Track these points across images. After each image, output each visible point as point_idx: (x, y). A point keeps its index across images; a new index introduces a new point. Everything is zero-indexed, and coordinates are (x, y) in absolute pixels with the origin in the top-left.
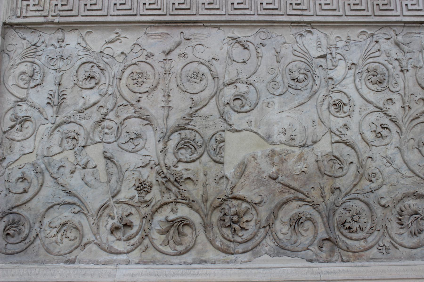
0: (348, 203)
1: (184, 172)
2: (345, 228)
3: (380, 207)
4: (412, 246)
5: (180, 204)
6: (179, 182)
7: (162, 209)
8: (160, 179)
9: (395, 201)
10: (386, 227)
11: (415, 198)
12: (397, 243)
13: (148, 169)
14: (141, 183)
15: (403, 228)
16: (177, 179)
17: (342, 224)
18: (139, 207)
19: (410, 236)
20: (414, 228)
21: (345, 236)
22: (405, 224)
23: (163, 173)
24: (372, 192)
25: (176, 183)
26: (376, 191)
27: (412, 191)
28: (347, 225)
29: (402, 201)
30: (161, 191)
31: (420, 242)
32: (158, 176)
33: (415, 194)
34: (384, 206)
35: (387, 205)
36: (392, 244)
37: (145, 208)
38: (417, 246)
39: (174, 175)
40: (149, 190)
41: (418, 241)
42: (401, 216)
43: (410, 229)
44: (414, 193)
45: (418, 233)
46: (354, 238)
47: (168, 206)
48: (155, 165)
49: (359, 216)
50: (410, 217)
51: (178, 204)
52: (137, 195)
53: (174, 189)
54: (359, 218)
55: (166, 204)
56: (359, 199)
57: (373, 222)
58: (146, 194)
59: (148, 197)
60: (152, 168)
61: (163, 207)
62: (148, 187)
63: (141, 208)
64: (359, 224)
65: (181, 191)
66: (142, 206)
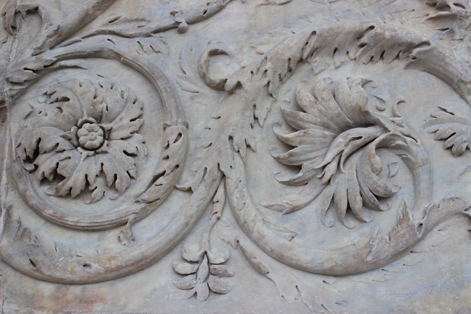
0: (70, 73)
2: (39, 174)
3: (207, 90)
4: (327, 265)
9: (269, 65)
10: (223, 176)
11: (365, 58)
12: (263, 249)
15: (303, 183)
17: (28, 160)
19: (330, 218)
20: (346, 184)
21: (37, 212)
22: (305, 165)
24: (175, 26)
26: (198, 27)
27: (351, 24)
28: (46, 163)
29: (305, 67)
31: (369, 246)
33: (364, 40)
34: (219, 87)
35: (230, 84)
36: (243, 251)
38: (352, 262)
41: (364, 241)
42: (295, 130)
43: (330, 190)
44: (359, 36)
45: (365, 204)
46: (71, 220)
49: (107, 126)
50: (335, 137)
54: (107, 135)
56: (117, 56)
57: (166, 153)
64: (101, 158)
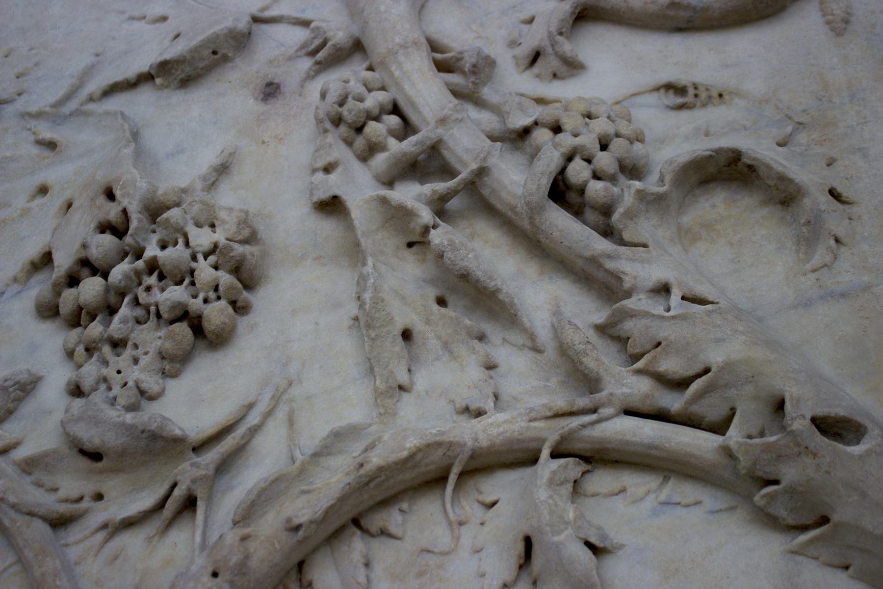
1: (652, 116)
5: (637, 483)
6: (607, 210)
7: (382, 550)
8: (359, 186)
13: (227, 99)
14: (118, 230)
16: (578, 171)
18: (60, 523)
23: (407, 128)
25: (559, 221)
30: (366, 323)
32: (339, 152)
37: (133, 542)
39: (542, 135)
40: (216, 314)
47: (469, 508)
48: (306, 64)
51: (602, 481)
52: (57, 377)
53: (542, 297)
55: (434, 474)
58: (173, 363)
59: (193, 402)
60: (270, 91)
61: (393, 519)
62: (205, 271)
63: (79, 541)
65: (638, 302)
66: (101, 514)
